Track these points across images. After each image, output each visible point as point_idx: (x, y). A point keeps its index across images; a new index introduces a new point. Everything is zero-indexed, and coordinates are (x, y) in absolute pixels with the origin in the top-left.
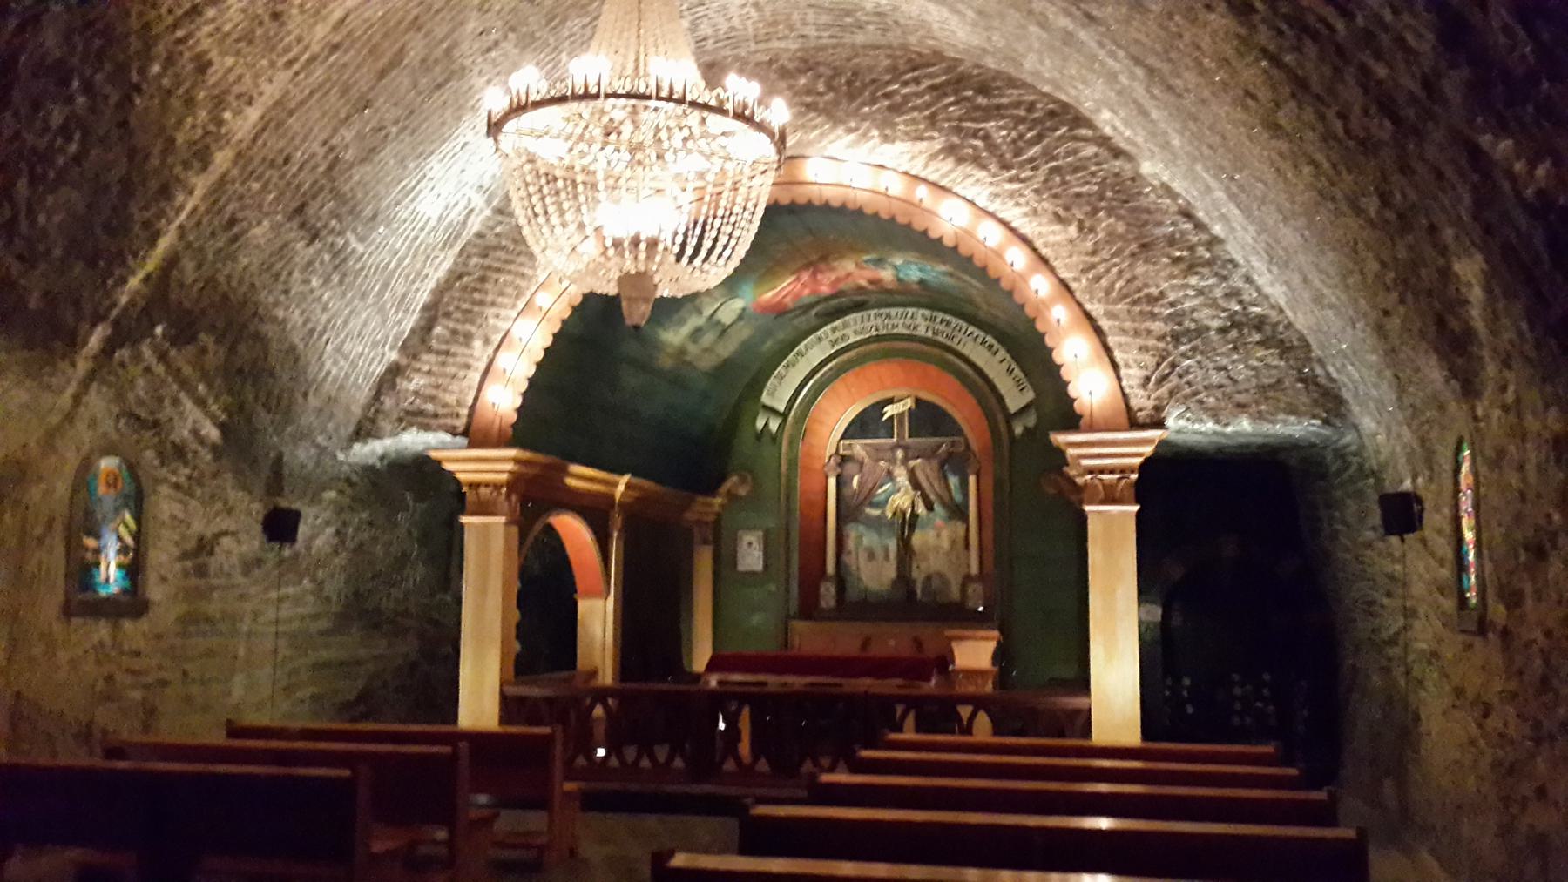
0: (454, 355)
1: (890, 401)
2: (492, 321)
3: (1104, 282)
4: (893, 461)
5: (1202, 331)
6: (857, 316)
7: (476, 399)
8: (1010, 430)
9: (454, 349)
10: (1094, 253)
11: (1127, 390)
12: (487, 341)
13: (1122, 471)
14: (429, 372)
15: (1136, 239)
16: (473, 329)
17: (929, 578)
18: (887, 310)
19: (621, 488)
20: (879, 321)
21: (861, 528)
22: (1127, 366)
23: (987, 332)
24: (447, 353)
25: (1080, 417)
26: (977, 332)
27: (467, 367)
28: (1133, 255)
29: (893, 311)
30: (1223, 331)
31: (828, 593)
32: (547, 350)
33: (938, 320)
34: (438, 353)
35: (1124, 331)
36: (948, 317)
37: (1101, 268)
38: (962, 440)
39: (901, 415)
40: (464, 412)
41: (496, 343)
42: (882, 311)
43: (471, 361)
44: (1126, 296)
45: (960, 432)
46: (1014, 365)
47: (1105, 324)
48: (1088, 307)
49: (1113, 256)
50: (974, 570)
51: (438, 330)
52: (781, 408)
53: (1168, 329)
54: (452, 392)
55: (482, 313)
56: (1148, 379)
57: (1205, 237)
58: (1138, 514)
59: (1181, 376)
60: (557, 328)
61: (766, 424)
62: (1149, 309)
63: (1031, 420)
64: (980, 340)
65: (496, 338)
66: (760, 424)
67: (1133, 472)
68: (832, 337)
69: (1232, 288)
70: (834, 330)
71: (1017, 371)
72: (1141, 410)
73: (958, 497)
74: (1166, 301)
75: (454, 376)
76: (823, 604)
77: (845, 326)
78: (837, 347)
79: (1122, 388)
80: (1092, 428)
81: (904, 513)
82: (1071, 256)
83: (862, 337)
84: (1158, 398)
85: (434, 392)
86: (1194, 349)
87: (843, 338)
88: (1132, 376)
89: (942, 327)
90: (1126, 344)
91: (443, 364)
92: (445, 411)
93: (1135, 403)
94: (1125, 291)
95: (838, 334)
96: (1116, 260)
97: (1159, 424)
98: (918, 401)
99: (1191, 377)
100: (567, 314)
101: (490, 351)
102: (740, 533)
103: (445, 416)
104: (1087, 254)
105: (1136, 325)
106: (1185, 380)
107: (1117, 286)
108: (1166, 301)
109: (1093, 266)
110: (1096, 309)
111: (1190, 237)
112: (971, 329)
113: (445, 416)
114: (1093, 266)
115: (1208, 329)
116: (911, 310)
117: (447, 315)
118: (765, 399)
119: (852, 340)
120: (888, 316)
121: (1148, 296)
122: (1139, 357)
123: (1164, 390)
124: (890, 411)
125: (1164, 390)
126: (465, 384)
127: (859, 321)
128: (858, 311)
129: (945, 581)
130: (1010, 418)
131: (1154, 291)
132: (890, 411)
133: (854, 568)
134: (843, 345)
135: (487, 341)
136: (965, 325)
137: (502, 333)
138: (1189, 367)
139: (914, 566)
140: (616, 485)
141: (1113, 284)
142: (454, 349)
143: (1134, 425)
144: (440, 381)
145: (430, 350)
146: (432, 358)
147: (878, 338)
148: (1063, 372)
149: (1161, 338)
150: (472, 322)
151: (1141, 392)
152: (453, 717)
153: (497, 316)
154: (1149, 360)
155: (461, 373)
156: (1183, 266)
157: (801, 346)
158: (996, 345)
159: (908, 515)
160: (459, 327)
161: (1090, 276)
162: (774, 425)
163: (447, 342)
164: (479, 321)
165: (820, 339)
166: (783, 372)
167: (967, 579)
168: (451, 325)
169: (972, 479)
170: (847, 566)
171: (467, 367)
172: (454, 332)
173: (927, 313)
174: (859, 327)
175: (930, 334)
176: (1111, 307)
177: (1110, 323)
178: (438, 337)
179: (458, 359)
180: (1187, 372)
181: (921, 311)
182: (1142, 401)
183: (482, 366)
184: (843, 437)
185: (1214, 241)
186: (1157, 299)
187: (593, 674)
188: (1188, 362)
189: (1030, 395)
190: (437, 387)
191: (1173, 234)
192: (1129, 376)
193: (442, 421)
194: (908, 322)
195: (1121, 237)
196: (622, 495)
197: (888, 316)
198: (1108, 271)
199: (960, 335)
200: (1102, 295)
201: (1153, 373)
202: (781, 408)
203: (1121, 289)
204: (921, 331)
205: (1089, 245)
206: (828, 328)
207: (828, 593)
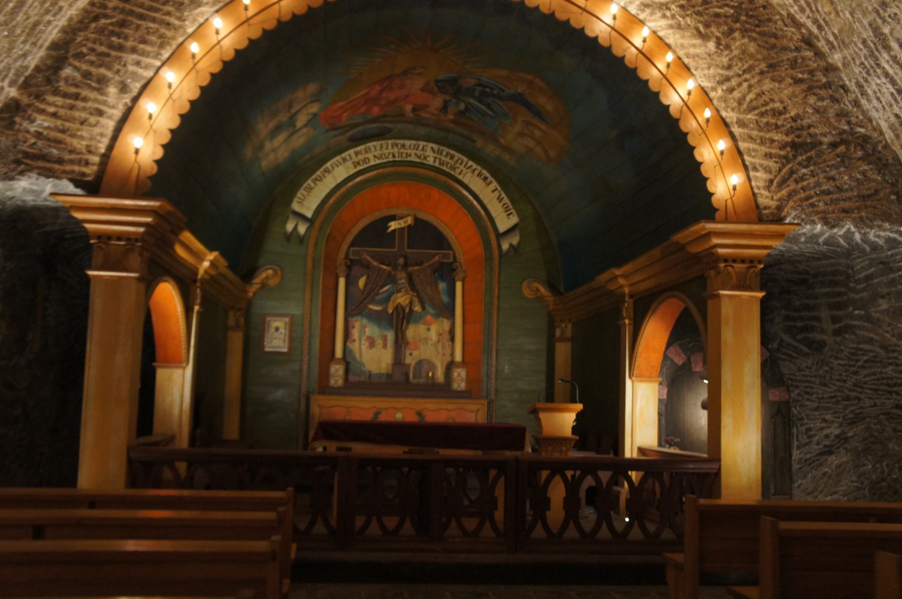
0: (85, 99)
1: (393, 218)
2: (131, 68)
3: (737, 94)
4: (395, 268)
5: (816, 144)
6: (377, 144)
7: (111, 147)
8: (499, 246)
9: (85, 93)
10: (729, 67)
11: (756, 191)
12: (124, 88)
13: (751, 261)
14: (55, 115)
15: (764, 59)
16: (109, 74)
17: (420, 363)
18: (402, 142)
19: (206, 264)
20: (396, 150)
21: (365, 321)
22: (755, 169)
23: (484, 167)
24: (76, 97)
25: (717, 210)
26: (475, 166)
27: (100, 113)
28: (762, 73)
29: (408, 143)
30: (834, 145)
31: (337, 371)
32: (192, 103)
33: (444, 153)
34: (65, 95)
35: (751, 139)
36: (452, 152)
37: (734, 82)
38: (451, 252)
39: (401, 230)
40: (96, 159)
41: (135, 92)
42: (398, 141)
43: (104, 108)
44: (754, 108)
45: (450, 248)
46: (503, 195)
47: (736, 130)
48: (724, 114)
49: (744, 72)
50: (458, 357)
51: (67, 71)
52: (309, 214)
53: (788, 139)
54: (82, 138)
55: (120, 58)
56: (771, 181)
57: (823, 64)
58: (763, 301)
59: (797, 182)
60: (205, 81)
61: (295, 228)
62: (774, 121)
63: (515, 240)
64: (476, 172)
65: (136, 86)
66: (290, 227)
67: (760, 262)
68: (355, 159)
69: (842, 110)
70: (357, 154)
71: (506, 200)
72: (765, 208)
73: (445, 299)
74: (788, 116)
75: (82, 123)
76: (332, 382)
77: (367, 151)
78: (360, 168)
79: (752, 188)
80: (726, 220)
81: (404, 310)
82: (709, 68)
83: (381, 161)
84: (780, 200)
85: (60, 136)
86: (809, 159)
87: (366, 160)
88: (760, 178)
89: (448, 159)
90: (754, 150)
91: (72, 108)
92: (73, 156)
93: (762, 201)
94: (755, 103)
95: (361, 157)
96: (747, 76)
97: (779, 220)
98: (416, 219)
99: (805, 183)
100: (217, 69)
101: (127, 99)
102: (268, 319)
103: (72, 162)
104: (723, 68)
105: (762, 134)
106: (800, 185)
107: (748, 99)
108: (788, 116)
109: (728, 79)
110: (730, 116)
111: (811, 63)
112: (470, 163)
113: (72, 162)
114: (728, 79)
115: (821, 143)
116: (422, 143)
117: (79, 56)
118: (295, 206)
119: (372, 163)
120: (403, 146)
121: (773, 110)
122: (765, 163)
123: (784, 192)
124: (393, 225)
125: (784, 192)
126: (97, 130)
127: (378, 148)
128: (378, 140)
129: (432, 367)
130: (500, 236)
131: (777, 105)
132: (393, 225)
133: (357, 355)
134: (365, 166)
135: (124, 88)
136: (465, 159)
137: (143, 82)
138: (804, 175)
139: (408, 352)
140: (201, 259)
141: (744, 97)
142: (85, 93)
143: (761, 220)
144: (68, 124)
145: (56, 92)
146: (59, 100)
147: (394, 163)
148: (703, 169)
149: (783, 146)
150: (109, 68)
151: (766, 193)
152: (72, 481)
153: (138, 63)
154: (779, 165)
155: (93, 120)
156: (804, 86)
157: (328, 165)
158: (490, 178)
159: (407, 310)
160: (93, 70)
161: (724, 88)
162: (302, 229)
163: (76, 86)
164: (117, 67)
165: (344, 160)
166: (312, 185)
167: (450, 367)
168: (84, 67)
169: (459, 285)
170: (351, 352)
171: (100, 113)
172: (87, 75)
173: (435, 146)
174: (378, 153)
175: (437, 164)
176: (741, 116)
177: (741, 130)
178: (66, 79)
179: (89, 104)
180: (802, 179)
181: (430, 145)
182: (766, 199)
183: (117, 113)
184: (352, 244)
185: (830, 69)
186: (780, 113)
187: (172, 438)
188: (804, 171)
189: (514, 220)
190: (63, 131)
191: (795, 60)
192: (757, 178)
193: (68, 168)
194: (419, 153)
195: (751, 56)
196: (206, 272)
197: (403, 146)
198: (740, 85)
199: (462, 167)
200: (735, 104)
201: (776, 176)
202: (309, 214)
203: (751, 101)
204: (430, 161)
205: (725, 60)
206: (352, 152)
207: (337, 371)
